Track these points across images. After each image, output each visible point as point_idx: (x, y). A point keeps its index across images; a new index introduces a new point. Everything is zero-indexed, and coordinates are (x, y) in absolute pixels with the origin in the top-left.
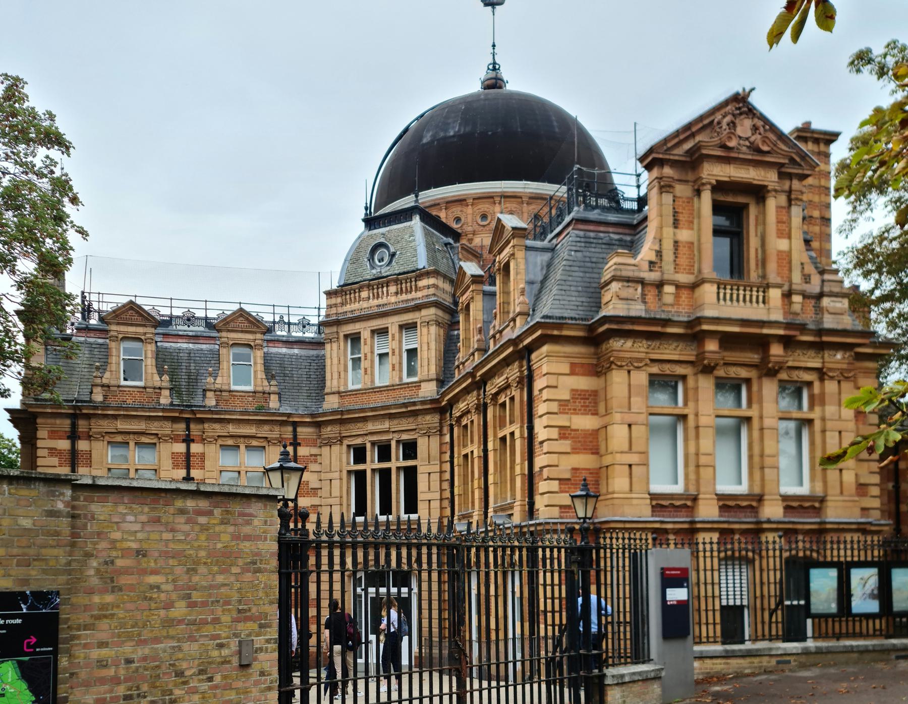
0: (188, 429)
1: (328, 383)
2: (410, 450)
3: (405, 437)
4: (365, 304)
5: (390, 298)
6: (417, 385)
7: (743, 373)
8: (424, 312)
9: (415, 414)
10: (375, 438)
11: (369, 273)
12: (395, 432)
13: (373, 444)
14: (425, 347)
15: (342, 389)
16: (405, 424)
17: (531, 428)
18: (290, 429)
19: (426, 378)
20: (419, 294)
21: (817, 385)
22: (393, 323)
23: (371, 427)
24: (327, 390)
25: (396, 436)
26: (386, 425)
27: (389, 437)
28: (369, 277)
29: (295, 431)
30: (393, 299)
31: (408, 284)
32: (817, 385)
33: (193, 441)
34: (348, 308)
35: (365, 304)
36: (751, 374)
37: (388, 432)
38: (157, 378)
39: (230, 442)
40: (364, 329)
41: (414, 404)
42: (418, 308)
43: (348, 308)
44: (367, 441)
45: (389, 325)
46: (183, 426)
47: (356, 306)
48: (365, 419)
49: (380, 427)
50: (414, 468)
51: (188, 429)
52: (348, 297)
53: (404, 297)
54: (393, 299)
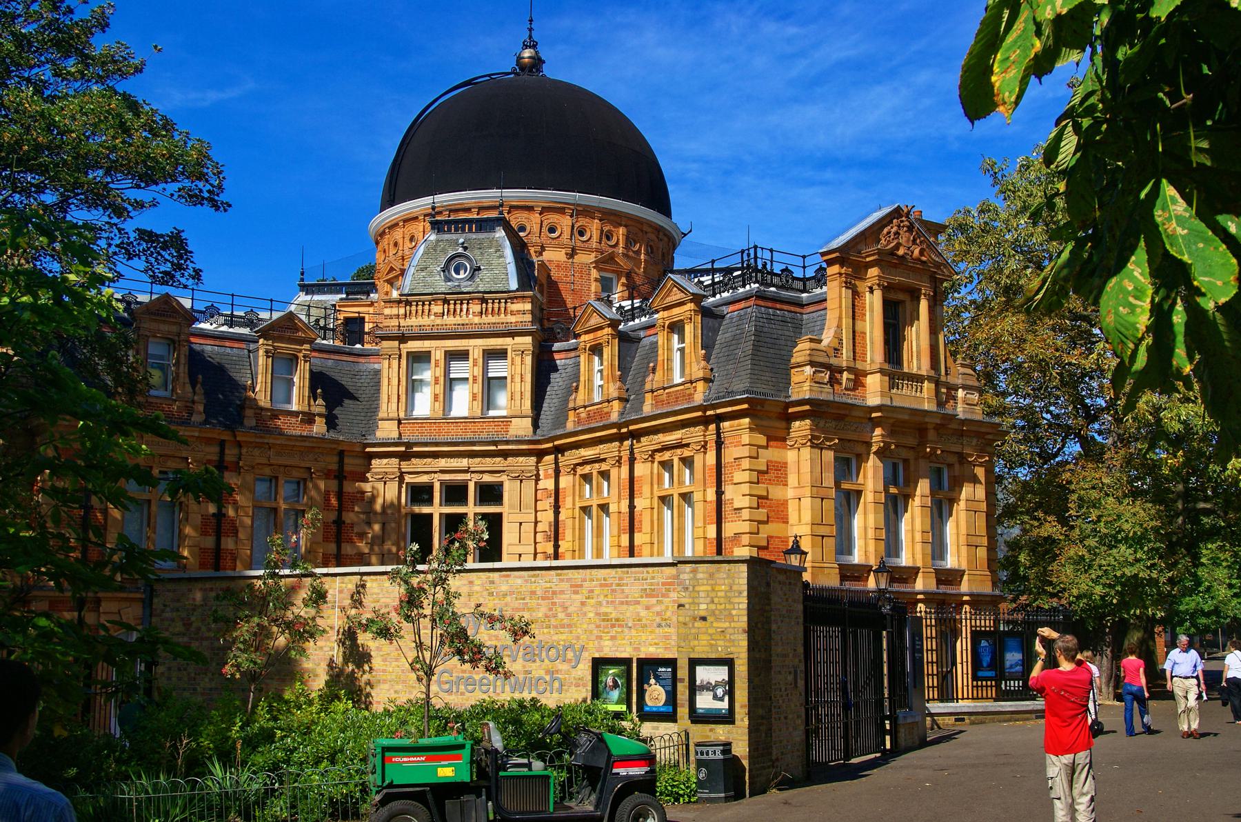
0: (222, 453)
1: (384, 406)
2: (491, 493)
3: (487, 478)
4: (439, 321)
5: (471, 316)
6: (506, 420)
7: (904, 454)
8: (518, 339)
9: (505, 454)
10: (447, 477)
11: (442, 286)
12: (474, 472)
13: (442, 483)
14: (518, 379)
15: (402, 415)
16: (489, 464)
17: (719, 493)
18: (336, 459)
19: (518, 413)
20: (512, 319)
21: (957, 466)
22: (476, 346)
23: (443, 463)
24: (382, 414)
25: (476, 477)
26: (464, 463)
27: (467, 476)
28: (443, 290)
29: (341, 462)
30: (477, 320)
31: (496, 305)
32: (957, 466)
33: (226, 468)
34: (413, 321)
35: (439, 321)
36: (910, 455)
37: (466, 471)
38: (189, 388)
39: (267, 471)
40: (438, 349)
41: (507, 442)
42: (512, 334)
43: (413, 321)
44: (437, 481)
45: (471, 349)
46: (215, 449)
47: (425, 321)
48: (435, 455)
49: (455, 464)
50: (499, 516)
51: (222, 453)
52: (414, 308)
53: (490, 319)
54: (477, 320)
